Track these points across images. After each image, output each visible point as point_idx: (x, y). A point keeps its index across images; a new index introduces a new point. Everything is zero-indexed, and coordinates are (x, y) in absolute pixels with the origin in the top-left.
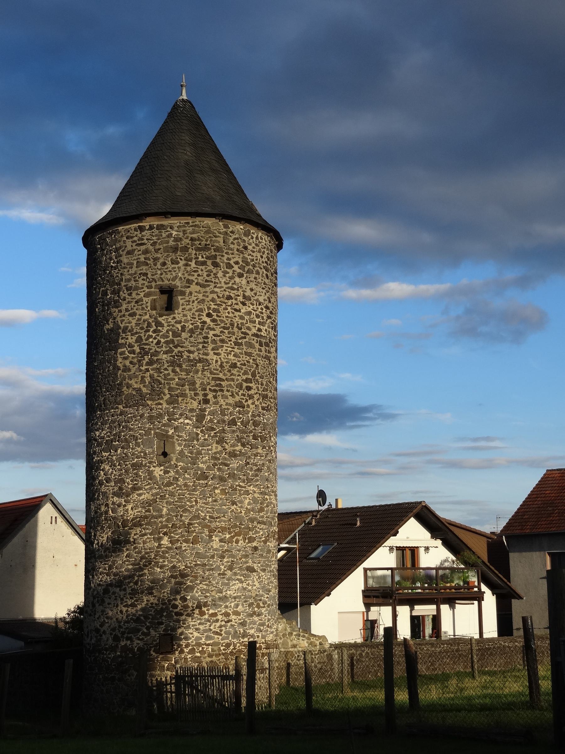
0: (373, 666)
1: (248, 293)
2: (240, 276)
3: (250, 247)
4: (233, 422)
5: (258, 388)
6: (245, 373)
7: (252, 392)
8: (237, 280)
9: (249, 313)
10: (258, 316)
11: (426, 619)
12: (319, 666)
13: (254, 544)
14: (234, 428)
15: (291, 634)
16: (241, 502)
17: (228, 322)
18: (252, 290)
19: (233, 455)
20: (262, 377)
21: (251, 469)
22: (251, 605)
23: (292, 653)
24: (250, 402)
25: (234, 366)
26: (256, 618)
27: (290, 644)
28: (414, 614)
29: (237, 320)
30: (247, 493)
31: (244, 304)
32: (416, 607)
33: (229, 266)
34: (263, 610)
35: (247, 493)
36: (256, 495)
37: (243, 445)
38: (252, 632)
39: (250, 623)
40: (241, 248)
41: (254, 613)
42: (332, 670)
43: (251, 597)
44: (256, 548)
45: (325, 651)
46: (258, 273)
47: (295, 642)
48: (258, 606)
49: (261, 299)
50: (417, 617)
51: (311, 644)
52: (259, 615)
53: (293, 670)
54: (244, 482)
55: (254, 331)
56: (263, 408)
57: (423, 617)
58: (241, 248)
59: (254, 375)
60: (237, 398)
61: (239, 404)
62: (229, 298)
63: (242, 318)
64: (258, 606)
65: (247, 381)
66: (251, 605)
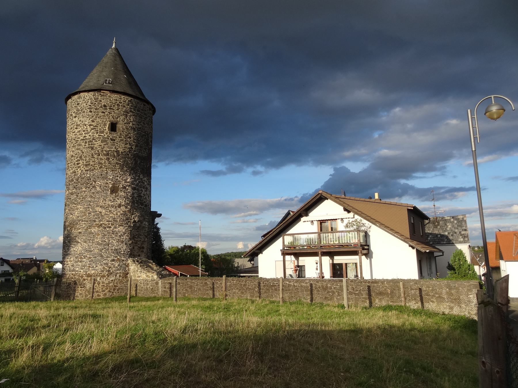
0: (183, 290)
1: (79, 123)
2: (75, 117)
3: (81, 103)
4: (72, 180)
5: (83, 163)
6: (77, 157)
7: (80, 165)
8: (74, 119)
9: (79, 131)
10: (84, 131)
11: (348, 265)
12: (151, 287)
13: (79, 231)
14: (73, 182)
15: (137, 271)
16: (74, 213)
17: (70, 138)
18: (80, 121)
19: (72, 194)
20: (86, 157)
21: (80, 199)
22: (76, 258)
23: (137, 280)
24: (79, 169)
25: (72, 156)
26: (80, 263)
27: (137, 275)
28: (335, 262)
29: (74, 136)
30: (77, 209)
31: (76, 128)
32: (336, 258)
33: (71, 115)
34: (84, 260)
35: (77, 209)
36: (81, 209)
37: (76, 189)
38: (77, 269)
39: (76, 265)
40: (76, 105)
41: (79, 261)
42: (158, 290)
43: (77, 254)
44: (80, 233)
45: (154, 280)
46: (84, 112)
47: (139, 275)
48: (81, 258)
49: (86, 123)
50: (341, 265)
51: (147, 276)
52: (81, 262)
53: (138, 287)
54: (75, 204)
55: (82, 138)
56: (86, 171)
57: (342, 264)
58: (76, 105)
59: (81, 157)
60: (74, 169)
61: (74, 172)
62: (72, 128)
63: (75, 135)
64: (81, 258)
65: (77, 161)
66: (76, 258)
